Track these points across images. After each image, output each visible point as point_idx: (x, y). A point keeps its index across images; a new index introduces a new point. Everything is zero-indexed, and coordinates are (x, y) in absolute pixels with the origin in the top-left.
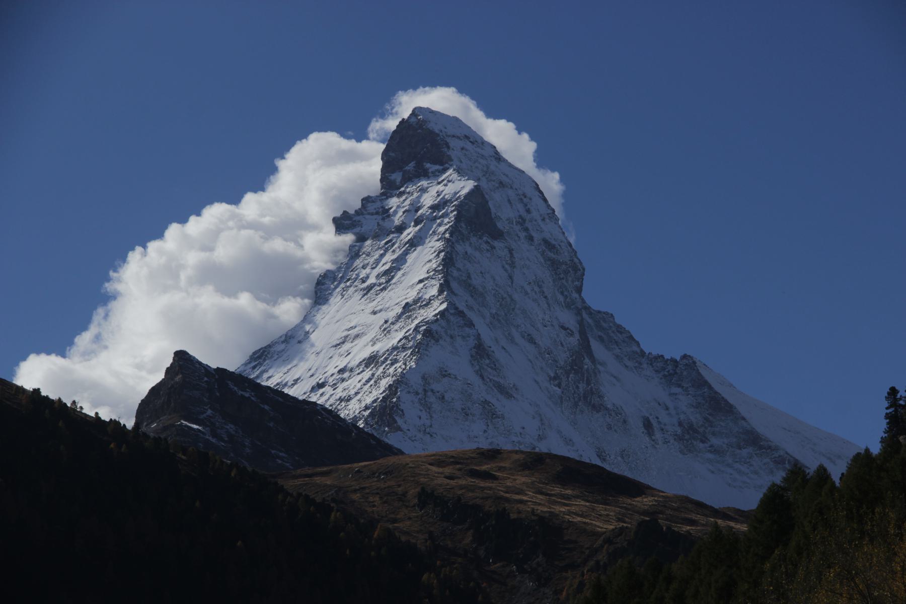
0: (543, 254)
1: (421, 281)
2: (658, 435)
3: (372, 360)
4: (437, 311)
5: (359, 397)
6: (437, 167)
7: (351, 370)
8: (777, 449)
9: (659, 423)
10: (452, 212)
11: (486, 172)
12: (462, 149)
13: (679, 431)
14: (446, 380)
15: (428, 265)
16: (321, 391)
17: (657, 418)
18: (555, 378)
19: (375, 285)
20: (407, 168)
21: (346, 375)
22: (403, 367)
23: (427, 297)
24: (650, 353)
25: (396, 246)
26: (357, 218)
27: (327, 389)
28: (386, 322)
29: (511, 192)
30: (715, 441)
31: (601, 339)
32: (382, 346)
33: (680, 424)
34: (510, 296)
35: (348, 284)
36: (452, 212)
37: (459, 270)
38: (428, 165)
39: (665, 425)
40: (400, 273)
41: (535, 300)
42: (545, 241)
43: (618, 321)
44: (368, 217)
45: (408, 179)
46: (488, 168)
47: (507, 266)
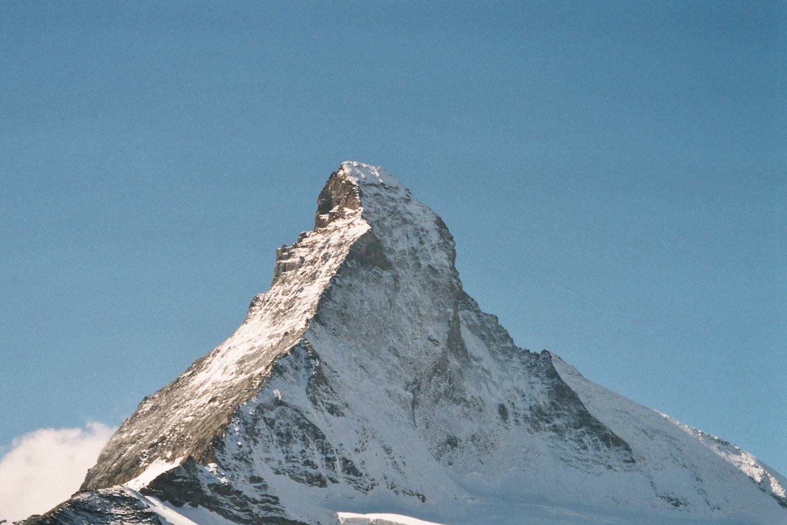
2: (511, 417)
8: (605, 428)
11: (392, 213)
12: (375, 195)
13: (529, 414)
14: (279, 408)
17: (513, 404)
18: (414, 383)
20: (332, 211)
29: (409, 228)
30: (557, 422)
33: (531, 408)
38: (346, 209)
42: (430, 266)
45: (334, 217)
46: (395, 208)
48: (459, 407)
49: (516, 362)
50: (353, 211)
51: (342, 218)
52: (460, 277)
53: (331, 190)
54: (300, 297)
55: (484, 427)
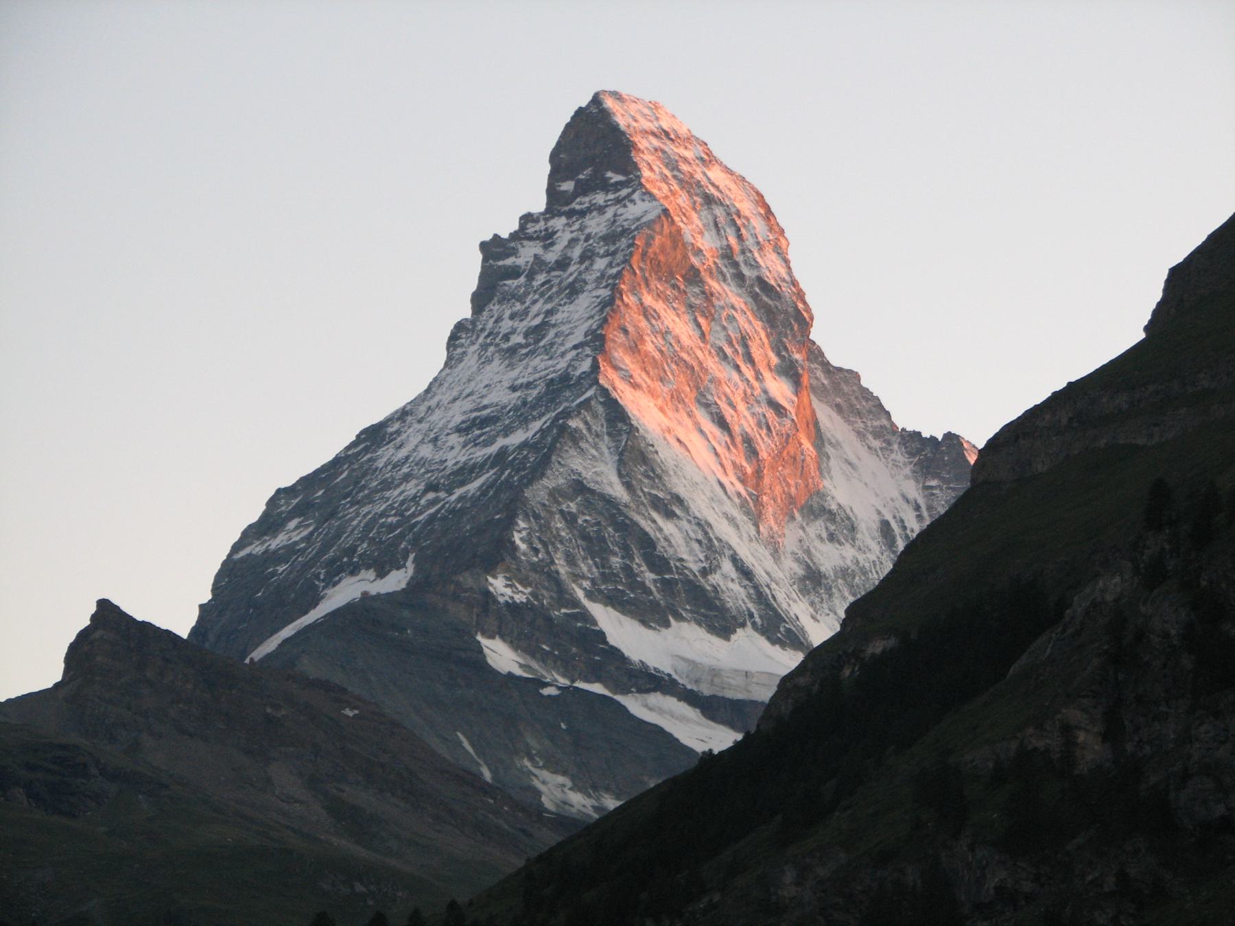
0: (755, 297)
1: (575, 347)
6: (620, 178)
9: (904, 528)
15: (591, 322)
17: (902, 521)
19: (520, 346)
23: (578, 373)
24: (903, 430)
25: (554, 290)
26: (512, 245)
27: (442, 495)
31: (839, 409)
34: (700, 363)
35: (488, 341)
37: (626, 332)
38: (609, 174)
41: (737, 368)
42: (761, 281)
43: (864, 383)
44: (525, 243)
45: (584, 189)
47: (701, 320)
49: (899, 456)
51: (602, 189)
52: (807, 298)
55: (861, 558)
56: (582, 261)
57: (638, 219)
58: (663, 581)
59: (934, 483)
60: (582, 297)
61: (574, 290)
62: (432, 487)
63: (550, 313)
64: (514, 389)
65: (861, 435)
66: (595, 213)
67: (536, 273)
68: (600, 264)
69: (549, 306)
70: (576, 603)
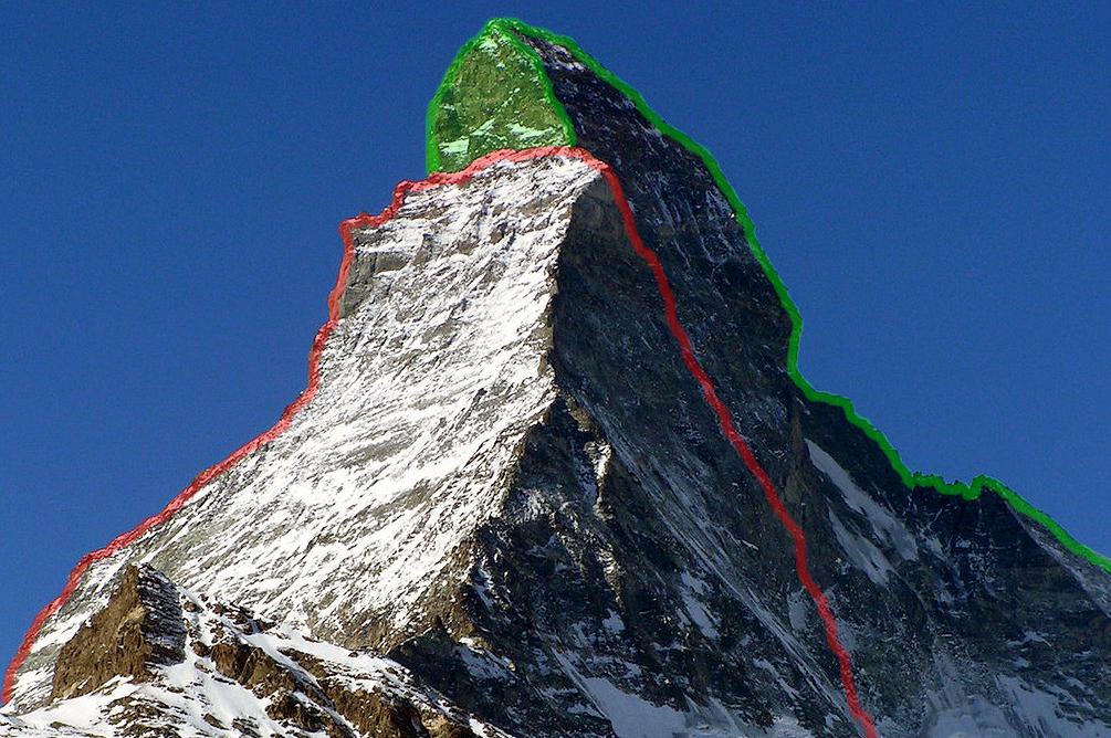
1: (507, 348)
3: (420, 493)
4: (538, 410)
5: (397, 565)
7: (380, 512)
9: (935, 604)
10: (561, 218)
16: (329, 548)
19: (422, 352)
21: (371, 522)
22: (478, 513)
25: (458, 279)
28: (443, 422)
30: (1031, 636)
31: (826, 445)
32: (434, 472)
36: (561, 218)
38: (516, 128)
39: (944, 605)
40: (464, 333)
44: (404, 221)
45: (479, 148)
48: (828, 593)
50: (540, 133)
53: (462, 85)
54: (466, 320)
56: (496, 237)
57: (571, 182)
58: (675, 653)
59: (965, 544)
60: (502, 285)
61: (491, 274)
62: (325, 540)
63: (464, 305)
64: (420, 405)
65: (862, 482)
66: (504, 178)
67: (428, 259)
68: (523, 241)
69: (455, 300)
70: (565, 681)
